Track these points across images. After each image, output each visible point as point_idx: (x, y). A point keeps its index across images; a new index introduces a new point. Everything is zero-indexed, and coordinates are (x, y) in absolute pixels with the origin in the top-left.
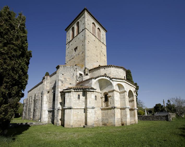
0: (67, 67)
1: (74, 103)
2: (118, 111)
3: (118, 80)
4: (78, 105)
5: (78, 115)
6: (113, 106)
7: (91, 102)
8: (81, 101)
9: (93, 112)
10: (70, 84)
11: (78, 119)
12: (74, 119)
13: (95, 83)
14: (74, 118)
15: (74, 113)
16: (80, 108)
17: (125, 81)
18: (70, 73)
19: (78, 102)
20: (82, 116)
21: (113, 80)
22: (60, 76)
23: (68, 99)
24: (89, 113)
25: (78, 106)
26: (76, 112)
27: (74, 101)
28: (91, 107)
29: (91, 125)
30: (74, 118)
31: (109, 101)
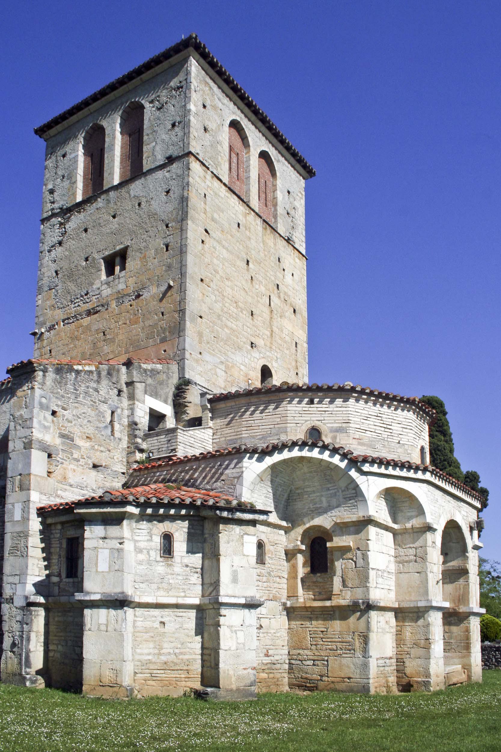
0: (78, 372)
1: (136, 574)
2: (383, 624)
3: (390, 471)
4: (165, 585)
6: (359, 595)
7: (241, 576)
8: (177, 569)
9: (250, 626)
11: (164, 658)
13: (261, 477)
15: (139, 624)
16: (173, 601)
17: (428, 476)
18: (94, 406)
19: (161, 568)
21: (366, 468)
22: (40, 422)
24: (230, 627)
25: (161, 593)
26: (148, 624)
27: (140, 563)
28: (243, 601)
29: (241, 685)
30: (138, 651)
31: (339, 572)
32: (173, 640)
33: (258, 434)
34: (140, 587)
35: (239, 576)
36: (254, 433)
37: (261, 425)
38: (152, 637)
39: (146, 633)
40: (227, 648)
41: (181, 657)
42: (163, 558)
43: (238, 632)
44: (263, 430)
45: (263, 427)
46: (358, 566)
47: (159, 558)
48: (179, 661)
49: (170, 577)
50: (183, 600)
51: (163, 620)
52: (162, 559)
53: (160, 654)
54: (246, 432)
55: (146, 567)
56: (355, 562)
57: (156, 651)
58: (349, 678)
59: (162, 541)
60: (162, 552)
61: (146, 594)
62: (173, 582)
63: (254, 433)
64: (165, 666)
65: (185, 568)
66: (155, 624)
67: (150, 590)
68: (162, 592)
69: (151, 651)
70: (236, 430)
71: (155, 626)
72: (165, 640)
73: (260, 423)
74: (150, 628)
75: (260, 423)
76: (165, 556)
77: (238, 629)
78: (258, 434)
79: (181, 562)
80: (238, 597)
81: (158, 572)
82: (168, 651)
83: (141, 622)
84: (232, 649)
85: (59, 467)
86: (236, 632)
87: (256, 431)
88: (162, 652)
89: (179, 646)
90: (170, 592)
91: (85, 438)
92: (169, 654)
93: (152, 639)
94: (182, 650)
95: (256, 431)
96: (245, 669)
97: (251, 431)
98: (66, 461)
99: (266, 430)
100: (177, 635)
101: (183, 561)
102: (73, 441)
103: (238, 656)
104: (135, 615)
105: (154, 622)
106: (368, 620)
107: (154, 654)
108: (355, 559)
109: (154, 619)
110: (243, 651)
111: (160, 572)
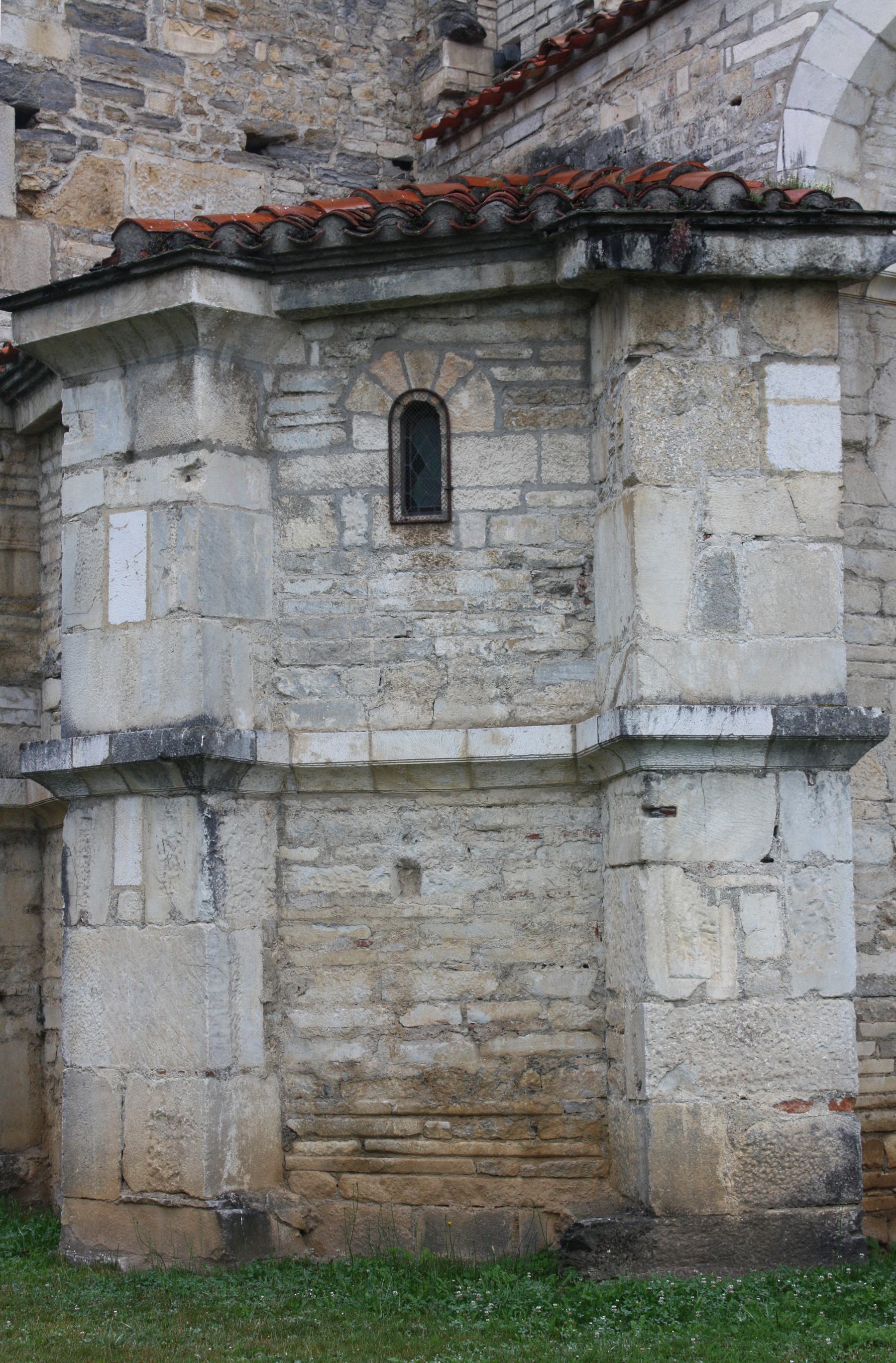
12: (296, 1054)
14: (301, 1018)
20: (506, 973)
32: (461, 953)
34: (301, 689)
35: (745, 587)
38: (362, 944)
39: (336, 922)
40: (685, 989)
41: (498, 1045)
42: (403, 531)
43: (747, 901)
47: (383, 534)
48: (491, 1065)
49: (435, 623)
50: (495, 740)
51: (410, 852)
52: (395, 538)
53: (401, 1033)
55: (329, 584)
57: (383, 1019)
59: (396, 445)
60: (397, 497)
61: (329, 722)
62: (454, 650)
64: (425, 1093)
65: (508, 574)
66: (375, 873)
67: (350, 700)
68: (402, 706)
69: (361, 1016)
71: (374, 888)
72: (422, 955)
76: (413, 518)
77: (744, 879)
79: (488, 544)
80: (732, 705)
81: (383, 603)
82: (437, 1013)
83: (310, 871)
84: (717, 994)
85: (74, 164)
86: (732, 897)
88: (411, 1019)
89: (491, 986)
90: (440, 705)
91: (202, 13)
92: (444, 1029)
93: (360, 953)
96: (791, 1106)
98: (113, 132)
100: (477, 928)
101: (494, 540)
102: (142, 37)
103: (750, 1033)
104: (281, 832)
105: (368, 864)
107: (375, 1034)
109: (366, 848)
110: (780, 1004)
111: (391, 601)
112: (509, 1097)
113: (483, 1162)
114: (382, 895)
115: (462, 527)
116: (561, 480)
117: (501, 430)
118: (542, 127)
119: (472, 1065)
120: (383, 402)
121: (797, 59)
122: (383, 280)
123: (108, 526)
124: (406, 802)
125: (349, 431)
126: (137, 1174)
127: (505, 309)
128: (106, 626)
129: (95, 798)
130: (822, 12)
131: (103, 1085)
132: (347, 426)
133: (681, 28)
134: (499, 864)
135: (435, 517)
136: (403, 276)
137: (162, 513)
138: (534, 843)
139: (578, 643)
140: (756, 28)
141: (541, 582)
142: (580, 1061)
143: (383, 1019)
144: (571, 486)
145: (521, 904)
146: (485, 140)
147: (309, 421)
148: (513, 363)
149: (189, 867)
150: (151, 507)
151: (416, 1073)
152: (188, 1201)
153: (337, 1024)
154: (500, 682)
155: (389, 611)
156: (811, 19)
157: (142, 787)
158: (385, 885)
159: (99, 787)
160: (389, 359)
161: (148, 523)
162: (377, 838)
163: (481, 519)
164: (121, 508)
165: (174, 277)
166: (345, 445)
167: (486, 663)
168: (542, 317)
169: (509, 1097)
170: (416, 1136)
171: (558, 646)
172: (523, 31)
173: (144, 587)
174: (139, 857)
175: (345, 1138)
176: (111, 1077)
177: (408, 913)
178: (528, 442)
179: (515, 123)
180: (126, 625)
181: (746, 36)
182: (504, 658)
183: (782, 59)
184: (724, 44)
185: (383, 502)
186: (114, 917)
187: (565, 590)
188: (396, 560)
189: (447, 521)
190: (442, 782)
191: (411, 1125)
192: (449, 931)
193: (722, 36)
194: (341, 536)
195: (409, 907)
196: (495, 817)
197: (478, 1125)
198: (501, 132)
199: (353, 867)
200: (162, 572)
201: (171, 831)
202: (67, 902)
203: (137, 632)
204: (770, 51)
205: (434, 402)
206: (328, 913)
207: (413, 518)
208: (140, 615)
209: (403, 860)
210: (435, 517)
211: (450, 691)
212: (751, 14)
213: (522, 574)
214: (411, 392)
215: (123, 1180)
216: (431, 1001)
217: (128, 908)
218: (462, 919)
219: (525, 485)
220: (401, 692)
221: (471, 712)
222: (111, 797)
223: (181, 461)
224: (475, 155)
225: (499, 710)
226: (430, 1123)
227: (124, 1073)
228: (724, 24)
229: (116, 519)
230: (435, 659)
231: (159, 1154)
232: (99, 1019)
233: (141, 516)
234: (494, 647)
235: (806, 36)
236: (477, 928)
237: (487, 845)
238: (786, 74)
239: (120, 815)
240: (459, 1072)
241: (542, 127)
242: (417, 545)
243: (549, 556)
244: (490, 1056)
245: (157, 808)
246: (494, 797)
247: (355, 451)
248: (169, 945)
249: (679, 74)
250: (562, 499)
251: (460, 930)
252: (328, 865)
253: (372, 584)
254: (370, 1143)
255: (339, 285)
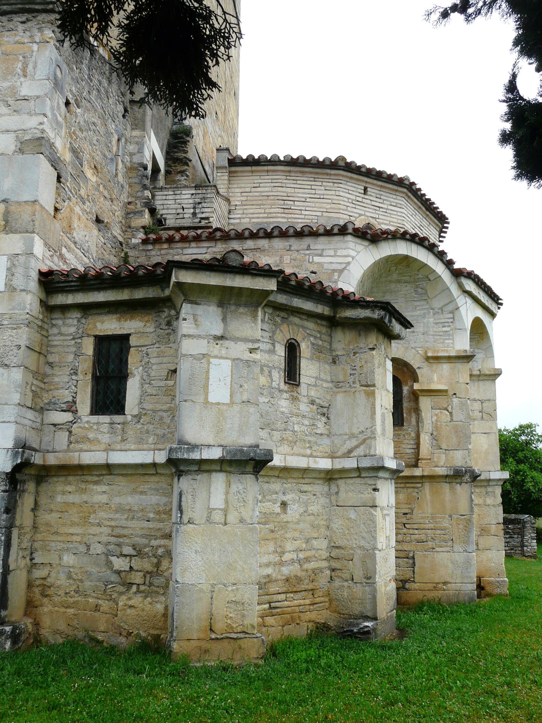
5: (284, 525)
10: (98, 221)
11: (286, 570)
16: (301, 463)
20: (307, 541)
23: (227, 365)
33: (300, 221)
36: (295, 218)
37: (304, 208)
38: (272, 531)
41: (306, 566)
44: (306, 217)
45: (307, 213)
46: (455, 419)
47: (283, 386)
48: (304, 574)
49: (294, 419)
50: (315, 462)
51: (285, 498)
53: (282, 563)
54: (283, 215)
56: (451, 413)
58: (445, 583)
62: (299, 429)
63: (295, 218)
70: (267, 211)
72: (288, 535)
73: (303, 206)
74: (270, 514)
75: (303, 206)
76: (290, 382)
78: (300, 221)
79: (307, 396)
81: (281, 409)
87: (297, 216)
90: (295, 448)
92: (293, 561)
93: (272, 535)
94: (308, 554)
95: (297, 216)
97: (290, 216)
99: (310, 217)
100: (302, 526)
106: (471, 497)
108: (450, 410)
109: (274, 496)
111: (284, 409)
112: (308, 584)
113: (301, 607)
114: (278, 514)
115: (302, 388)
116: (324, 378)
117: (312, 359)
118: (206, 253)
119: (299, 574)
120: (283, 340)
121: (344, 269)
122: (296, 300)
123: (209, 363)
124: (285, 481)
125: (274, 347)
126: (219, 626)
127: (313, 320)
128: (206, 402)
129: (200, 471)
130: (353, 259)
131: (201, 590)
132: (274, 345)
133: (287, 244)
134: (306, 504)
135: (295, 383)
136: (300, 300)
137: (241, 365)
138: (315, 497)
139: (327, 432)
140: (324, 254)
141: (319, 411)
142: (324, 570)
143: (274, 558)
144: (326, 381)
145: (312, 517)
146: (170, 248)
147: (264, 340)
148: (315, 337)
149: (251, 502)
150: (234, 360)
151: (284, 578)
152: (247, 636)
153: (265, 561)
154: (309, 442)
155: (283, 413)
156: (350, 259)
157: (228, 469)
158: (278, 510)
159: (205, 467)
160: (285, 326)
161: (232, 366)
162: (277, 493)
163: (305, 386)
164: (216, 357)
165: (267, 279)
166: (272, 351)
167: (307, 435)
168: (322, 325)
169: (308, 584)
170: (284, 601)
171: (323, 432)
172: (168, 217)
173: (229, 390)
174: (224, 497)
175: (265, 604)
176: (206, 587)
177: (285, 520)
178: (317, 364)
179: (189, 247)
180: (218, 404)
181: (321, 255)
182: (311, 434)
183: (340, 267)
184: (309, 255)
185: (283, 374)
186: (209, 520)
187: (324, 415)
188: (285, 395)
189: (298, 385)
190: (296, 475)
191: (283, 596)
192: (294, 526)
193: (308, 252)
194: (272, 384)
195: (284, 518)
196: (305, 488)
197: (299, 595)
198: (182, 249)
199: (271, 503)
200: (239, 386)
201: (241, 487)
202: (182, 513)
203: (225, 407)
204: (331, 263)
205: (296, 344)
206: (263, 520)
207: (290, 382)
208: (227, 400)
209: (283, 501)
210: (295, 383)
211: (298, 443)
212: (323, 250)
213: (315, 407)
214: (291, 339)
215: (211, 629)
216: (290, 552)
217: (218, 517)
218: (297, 523)
219: (316, 378)
220: (286, 442)
221: (302, 451)
222: (209, 471)
223: (251, 346)
224: (163, 252)
225: (308, 452)
226: (288, 595)
227: (213, 586)
228: (308, 248)
229: (212, 360)
230: (294, 431)
231: (231, 617)
232: (200, 563)
233: (229, 362)
234: (308, 430)
235: (349, 263)
236: (302, 526)
237: (304, 497)
238: (341, 271)
239: (213, 479)
240: (296, 576)
241: (206, 253)
242: (291, 391)
243: (321, 403)
244: (303, 570)
245: (234, 478)
246: (306, 481)
247: (276, 354)
248: (239, 533)
249: (285, 257)
250: (325, 385)
251: (297, 526)
252: (264, 502)
253: (279, 403)
254: (273, 605)
255: (285, 297)
